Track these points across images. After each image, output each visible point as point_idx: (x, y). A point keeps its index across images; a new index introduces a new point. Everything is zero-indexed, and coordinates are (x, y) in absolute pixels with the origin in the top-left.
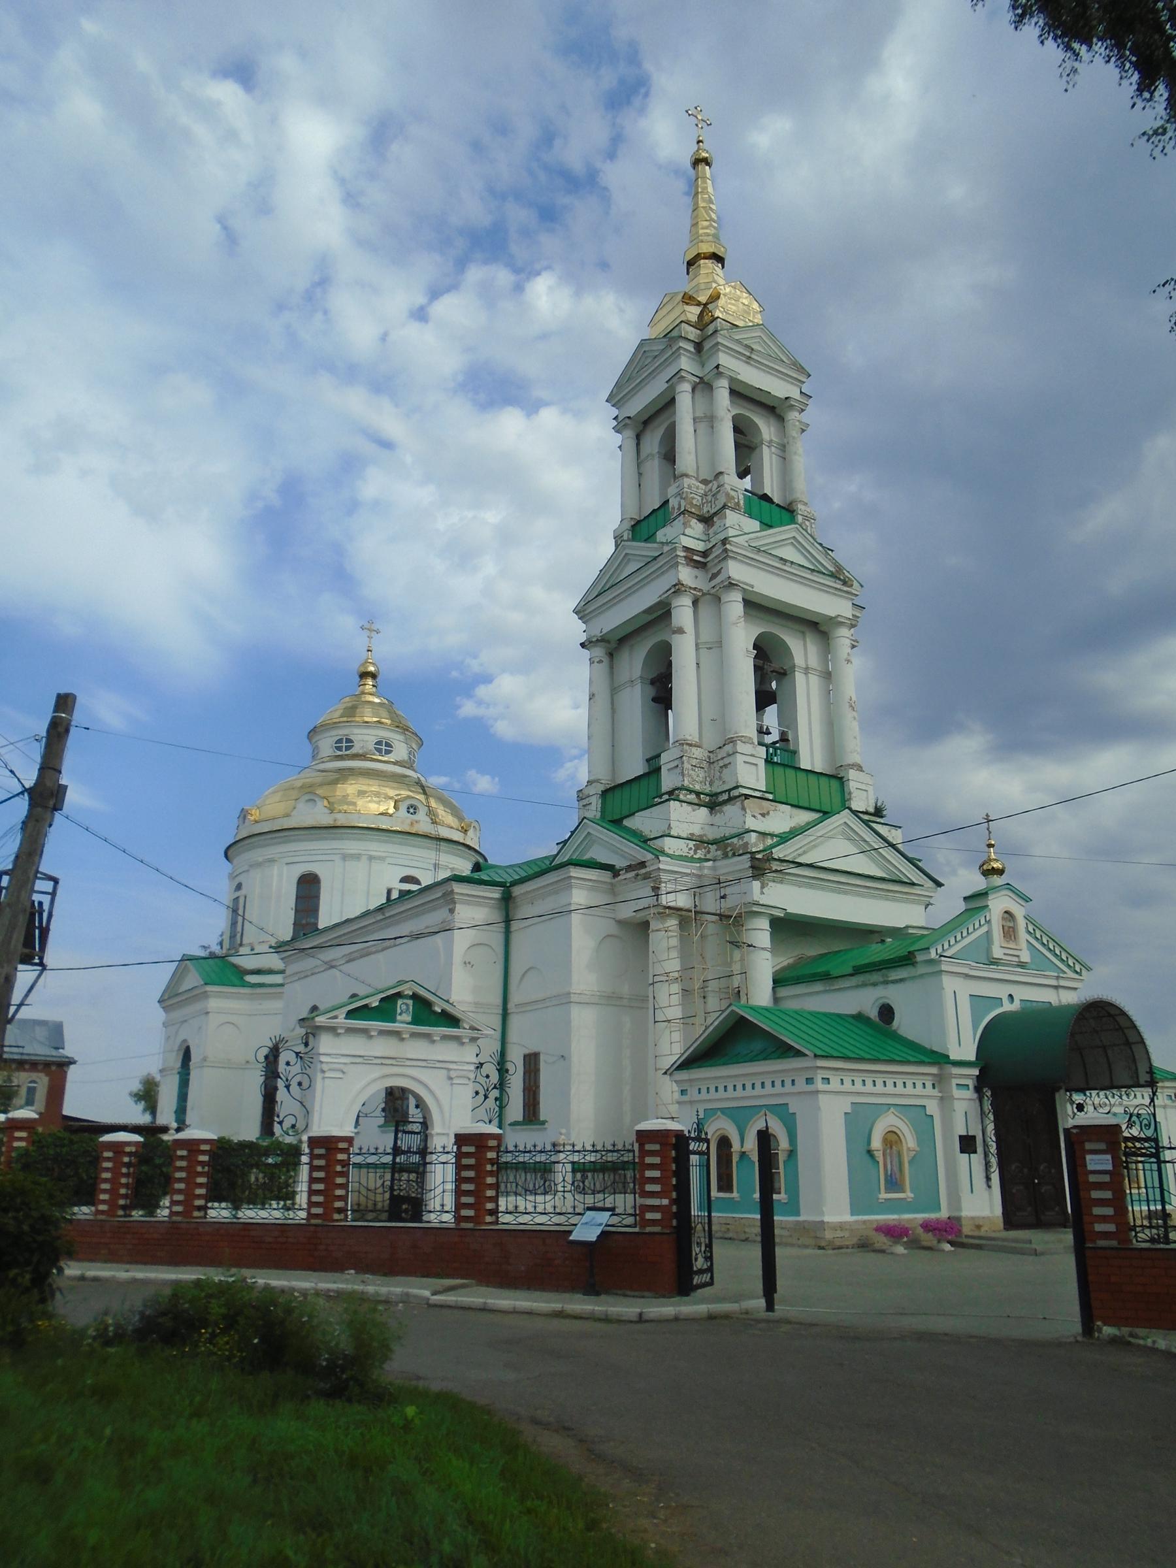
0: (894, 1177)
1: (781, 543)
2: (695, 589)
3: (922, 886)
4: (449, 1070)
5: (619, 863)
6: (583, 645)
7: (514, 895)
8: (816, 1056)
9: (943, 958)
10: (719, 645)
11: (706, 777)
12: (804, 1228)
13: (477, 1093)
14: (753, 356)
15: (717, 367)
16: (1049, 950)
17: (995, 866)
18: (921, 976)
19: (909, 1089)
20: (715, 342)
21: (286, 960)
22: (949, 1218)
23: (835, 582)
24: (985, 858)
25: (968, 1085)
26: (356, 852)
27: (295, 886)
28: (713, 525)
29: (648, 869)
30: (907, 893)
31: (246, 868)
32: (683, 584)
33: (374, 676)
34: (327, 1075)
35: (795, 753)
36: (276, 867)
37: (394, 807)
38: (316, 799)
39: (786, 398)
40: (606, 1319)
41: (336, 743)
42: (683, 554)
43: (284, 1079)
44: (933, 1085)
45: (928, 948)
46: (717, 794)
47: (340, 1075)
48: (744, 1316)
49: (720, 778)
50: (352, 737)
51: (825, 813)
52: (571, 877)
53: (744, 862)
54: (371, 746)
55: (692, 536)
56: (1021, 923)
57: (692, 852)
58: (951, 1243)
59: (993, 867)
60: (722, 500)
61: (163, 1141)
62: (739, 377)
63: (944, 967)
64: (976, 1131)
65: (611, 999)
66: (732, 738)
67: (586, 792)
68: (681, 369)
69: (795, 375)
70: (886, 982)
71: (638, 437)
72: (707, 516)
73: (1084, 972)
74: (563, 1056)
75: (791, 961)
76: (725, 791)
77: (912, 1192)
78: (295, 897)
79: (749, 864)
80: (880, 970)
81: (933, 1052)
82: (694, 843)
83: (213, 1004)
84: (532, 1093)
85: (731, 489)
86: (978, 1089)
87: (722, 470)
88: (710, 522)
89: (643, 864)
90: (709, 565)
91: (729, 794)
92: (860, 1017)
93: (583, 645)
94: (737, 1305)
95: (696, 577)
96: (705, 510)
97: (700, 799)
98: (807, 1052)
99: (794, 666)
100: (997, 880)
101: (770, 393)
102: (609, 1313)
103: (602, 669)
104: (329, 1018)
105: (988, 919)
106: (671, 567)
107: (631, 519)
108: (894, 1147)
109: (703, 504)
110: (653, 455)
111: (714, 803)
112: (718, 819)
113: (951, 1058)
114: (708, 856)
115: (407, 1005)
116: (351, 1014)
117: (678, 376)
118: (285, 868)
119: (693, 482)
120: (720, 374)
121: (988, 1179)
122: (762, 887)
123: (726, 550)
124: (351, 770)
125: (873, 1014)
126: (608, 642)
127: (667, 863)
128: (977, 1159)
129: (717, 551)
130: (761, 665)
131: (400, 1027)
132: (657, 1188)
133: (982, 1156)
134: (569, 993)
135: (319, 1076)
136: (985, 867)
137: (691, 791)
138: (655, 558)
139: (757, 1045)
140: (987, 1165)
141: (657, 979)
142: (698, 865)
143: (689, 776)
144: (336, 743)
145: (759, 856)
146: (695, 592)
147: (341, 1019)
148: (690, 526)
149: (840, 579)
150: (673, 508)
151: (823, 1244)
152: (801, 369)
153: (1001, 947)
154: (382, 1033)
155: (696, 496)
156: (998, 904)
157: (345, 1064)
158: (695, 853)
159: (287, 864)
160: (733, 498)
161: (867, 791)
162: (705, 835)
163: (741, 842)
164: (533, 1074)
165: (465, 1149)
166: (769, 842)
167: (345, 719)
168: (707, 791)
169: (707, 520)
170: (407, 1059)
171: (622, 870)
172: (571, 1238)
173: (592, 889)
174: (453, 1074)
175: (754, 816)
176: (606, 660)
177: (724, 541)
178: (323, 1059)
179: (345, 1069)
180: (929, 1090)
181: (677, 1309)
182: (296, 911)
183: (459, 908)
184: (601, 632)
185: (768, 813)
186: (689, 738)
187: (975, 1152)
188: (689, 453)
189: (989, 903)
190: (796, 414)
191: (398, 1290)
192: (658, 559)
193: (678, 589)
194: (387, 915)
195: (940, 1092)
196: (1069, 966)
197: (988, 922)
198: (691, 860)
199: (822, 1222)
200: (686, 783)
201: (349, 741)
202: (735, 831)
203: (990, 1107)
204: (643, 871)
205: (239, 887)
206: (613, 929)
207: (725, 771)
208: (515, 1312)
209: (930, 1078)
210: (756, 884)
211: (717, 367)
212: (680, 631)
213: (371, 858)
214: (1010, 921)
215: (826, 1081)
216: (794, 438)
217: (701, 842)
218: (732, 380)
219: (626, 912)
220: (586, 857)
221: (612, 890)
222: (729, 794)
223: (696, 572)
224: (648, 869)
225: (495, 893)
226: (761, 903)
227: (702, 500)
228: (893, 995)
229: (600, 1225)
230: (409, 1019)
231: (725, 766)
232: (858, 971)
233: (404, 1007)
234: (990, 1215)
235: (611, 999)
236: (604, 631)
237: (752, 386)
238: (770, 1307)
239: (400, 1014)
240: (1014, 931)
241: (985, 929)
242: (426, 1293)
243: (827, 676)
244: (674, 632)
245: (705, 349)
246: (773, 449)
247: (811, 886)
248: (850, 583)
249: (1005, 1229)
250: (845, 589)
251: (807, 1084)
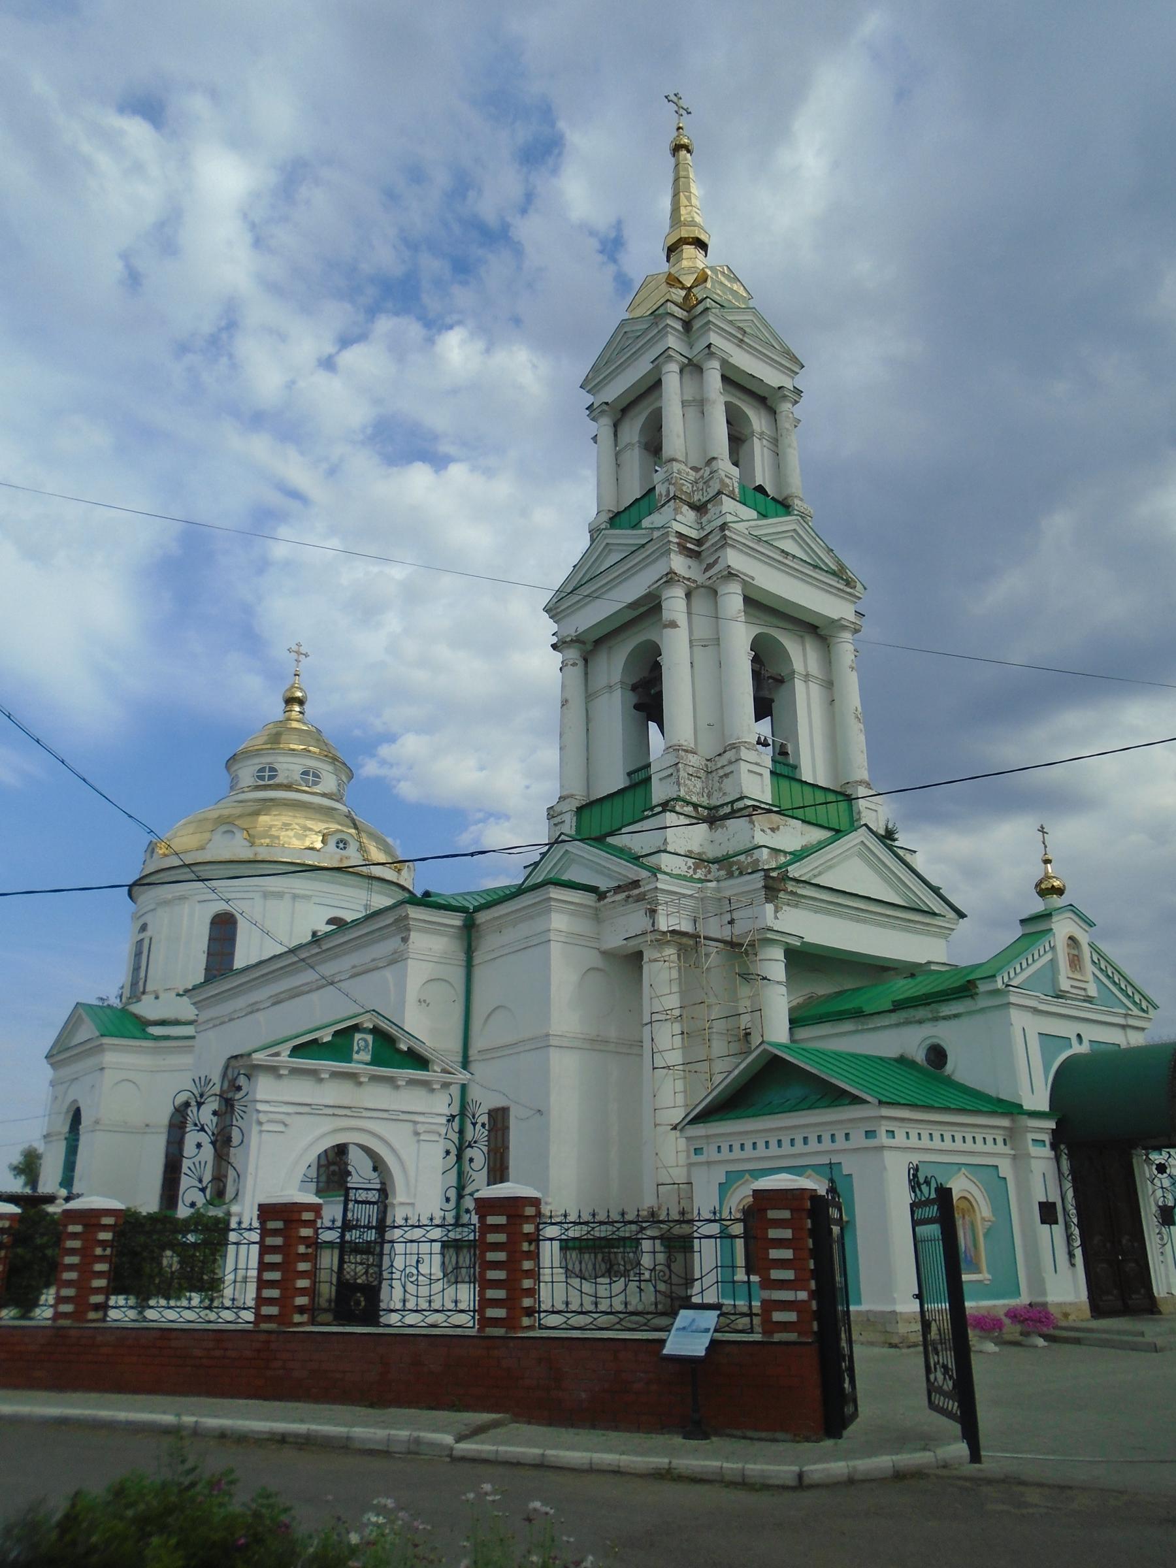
0: (968, 1255)
1: (780, 536)
2: (689, 579)
3: (944, 916)
4: (415, 1123)
5: (603, 884)
6: (554, 647)
7: (478, 922)
8: (880, 1102)
9: (1011, 988)
10: (716, 641)
11: (703, 789)
12: (868, 1320)
13: (448, 1153)
15: (709, 346)
16: (1114, 983)
17: (1055, 884)
18: (982, 1010)
19: (980, 1146)
20: (705, 321)
21: (200, 1005)
22: (1030, 1305)
23: (838, 582)
24: (1042, 875)
25: (1044, 1141)
26: (280, 889)
27: (208, 926)
28: (706, 513)
29: (642, 890)
30: (928, 924)
31: (152, 907)
32: (676, 573)
33: (301, 702)
34: (265, 1127)
35: (795, 767)
36: (186, 906)
37: (323, 842)
38: (235, 830)
39: (779, 388)
40: (743, 1484)
41: (258, 772)
42: (676, 540)
43: (210, 1133)
44: (1004, 1140)
45: (994, 976)
46: (716, 808)
47: (281, 1128)
48: (944, 1472)
49: (720, 789)
50: (276, 766)
51: (838, 831)
52: (550, 899)
53: (757, 880)
54: (297, 777)
55: (685, 522)
56: (1086, 950)
57: (691, 871)
58: (1046, 1337)
59: (1053, 886)
60: (715, 486)
61: (48, 1214)
62: (731, 360)
63: (1013, 999)
64: (1054, 1197)
65: (595, 1044)
66: (734, 744)
67: (558, 809)
68: (669, 348)
69: (788, 365)
70: (936, 1019)
71: (616, 426)
72: (698, 504)
73: (1151, 1009)
74: (539, 1111)
75: (800, 1000)
76: (727, 804)
77: (989, 1272)
78: (207, 938)
79: (762, 883)
80: (929, 1004)
81: (1000, 1101)
82: (694, 860)
83: (109, 1058)
84: (498, 1155)
85: (726, 476)
86: (1054, 1146)
87: (716, 456)
88: (703, 510)
89: (636, 884)
90: (704, 554)
91: (732, 806)
92: (903, 1061)
93: (554, 647)
94: (928, 1454)
95: (690, 567)
96: (696, 498)
97: (698, 813)
98: (869, 1099)
99: (793, 672)
100: (1056, 901)
101: (762, 380)
102: (747, 1473)
103: (576, 672)
104: (268, 1056)
105: (1052, 945)
106: (662, 554)
107: (609, 511)
108: (966, 1217)
109: (693, 492)
110: (633, 445)
111: (713, 817)
112: (719, 834)
113: (1025, 1108)
114: (709, 877)
115: (365, 1041)
116: (296, 1051)
117: (665, 355)
118: (198, 907)
119: (683, 467)
120: (711, 355)
121: (1071, 1255)
122: (776, 911)
123: (725, 537)
124: (272, 800)
125: (920, 1057)
126: (584, 643)
127: (665, 882)
128: (1058, 1230)
129: (713, 539)
130: (758, 669)
131: (356, 1068)
132: (789, 1275)
133: (1063, 1227)
134: (548, 1035)
135: (255, 1129)
136: (1043, 886)
137: (688, 803)
138: (643, 546)
139: (796, 1092)
140: (1069, 1238)
141: (656, 1017)
142: (700, 885)
143: (686, 785)
144: (258, 772)
145: (774, 874)
146: (688, 583)
147: (284, 1057)
148: (681, 513)
149: (843, 579)
150: (661, 495)
151: (895, 1340)
152: (794, 359)
153: (1068, 978)
154: (335, 1075)
155: (685, 483)
156: (1063, 927)
157: (288, 1114)
158: (695, 873)
159: (199, 902)
160: (728, 486)
161: (876, 811)
162: (704, 853)
163: (749, 860)
164: (500, 1133)
165: (491, 1220)
166: (782, 859)
167: (269, 746)
168: (705, 804)
169: (700, 509)
170: (366, 1109)
171: (608, 892)
172: (665, 1352)
173: (573, 914)
174: (420, 1128)
175: (763, 831)
176: (581, 663)
177: (723, 527)
178: (260, 1107)
179: (288, 1120)
180: (1000, 1147)
181: (851, 1463)
182: (209, 954)
183: (414, 936)
184: (576, 631)
185: (778, 828)
186: (685, 743)
187: (1056, 1223)
188: (678, 436)
189: (1053, 926)
190: (790, 405)
191: (404, 1434)
192: (647, 546)
193: (670, 578)
194: (324, 947)
195: (1012, 1149)
196: (1135, 1003)
197: (1053, 948)
198: (691, 879)
199: (894, 1313)
200: (682, 794)
201: (272, 769)
202: (742, 847)
204: (636, 892)
205: (144, 928)
206: (595, 960)
207: (725, 780)
208: (592, 1470)
209: (1001, 1132)
210: (769, 908)
211: (709, 346)
212: (673, 625)
213: (295, 897)
214: (1074, 948)
215: (890, 1134)
216: (788, 430)
217: (701, 860)
218: (725, 363)
219: (614, 940)
220: (565, 877)
221: (597, 917)
222: (732, 806)
223: (689, 561)
224: (642, 890)
225: (456, 920)
226: (775, 929)
227: (693, 487)
228: (945, 1033)
229: (707, 1330)
230: (368, 1058)
231: (726, 775)
232: (899, 1006)
233: (362, 1043)
234: (1076, 1300)
235: (595, 1044)
236: (580, 630)
237: (744, 371)
238: (975, 1457)
239: (357, 1052)
240: (1079, 960)
241: (1049, 956)
242: (448, 1439)
243: (829, 684)
244: (666, 626)
245: (694, 329)
246: (765, 442)
247: (828, 913)
248: (853, 584)
249: (1092, 1317)
250: (849, 590)
251: (866, 1138)
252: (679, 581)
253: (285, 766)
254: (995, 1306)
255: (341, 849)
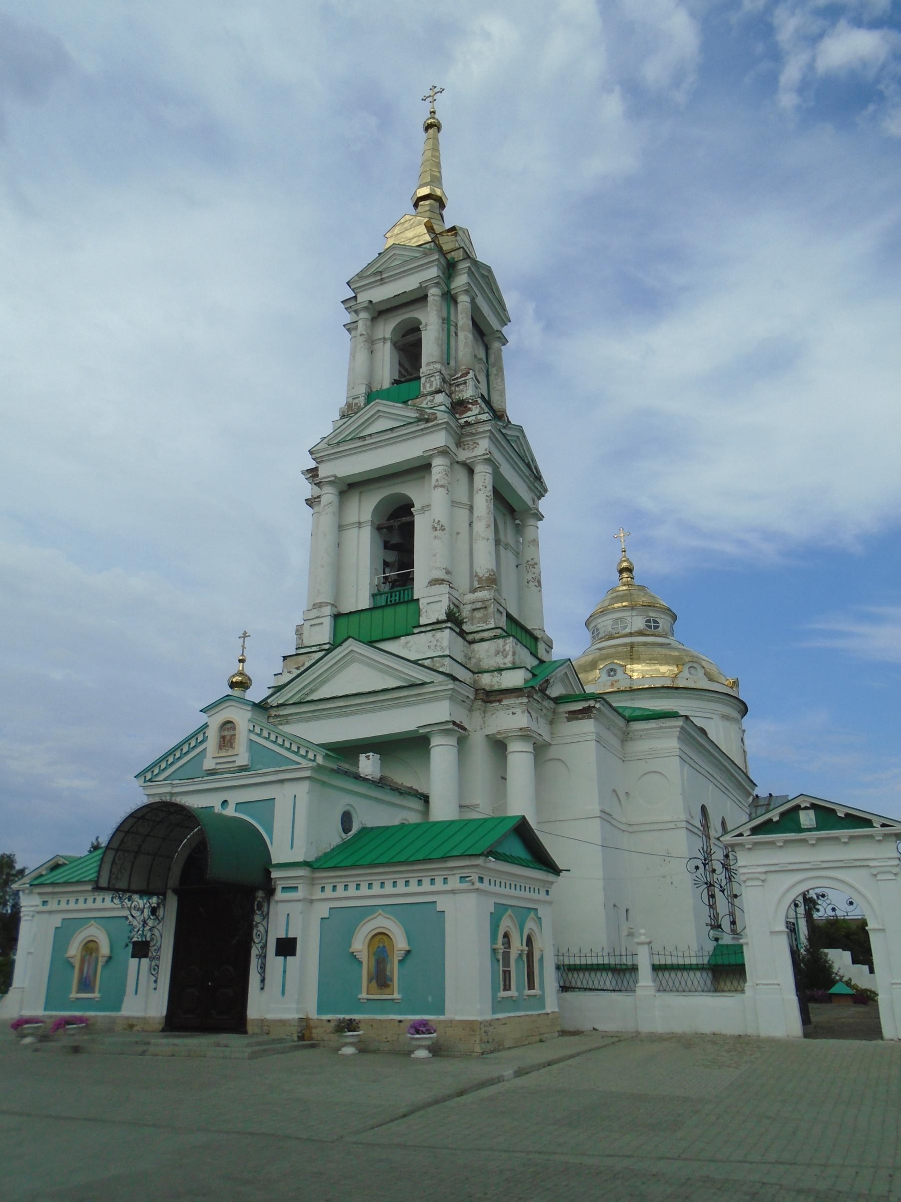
14: (384, 276)
23: (418, 425)
69: (426, 261)
101: (405, 292)
108: (94, 955)
203: (150, 913)
247: (317, 718)
250: (430, 424)
252: (312, 503)
253: (602, 624)
254: (96, 1016)
255: (612, 676)
